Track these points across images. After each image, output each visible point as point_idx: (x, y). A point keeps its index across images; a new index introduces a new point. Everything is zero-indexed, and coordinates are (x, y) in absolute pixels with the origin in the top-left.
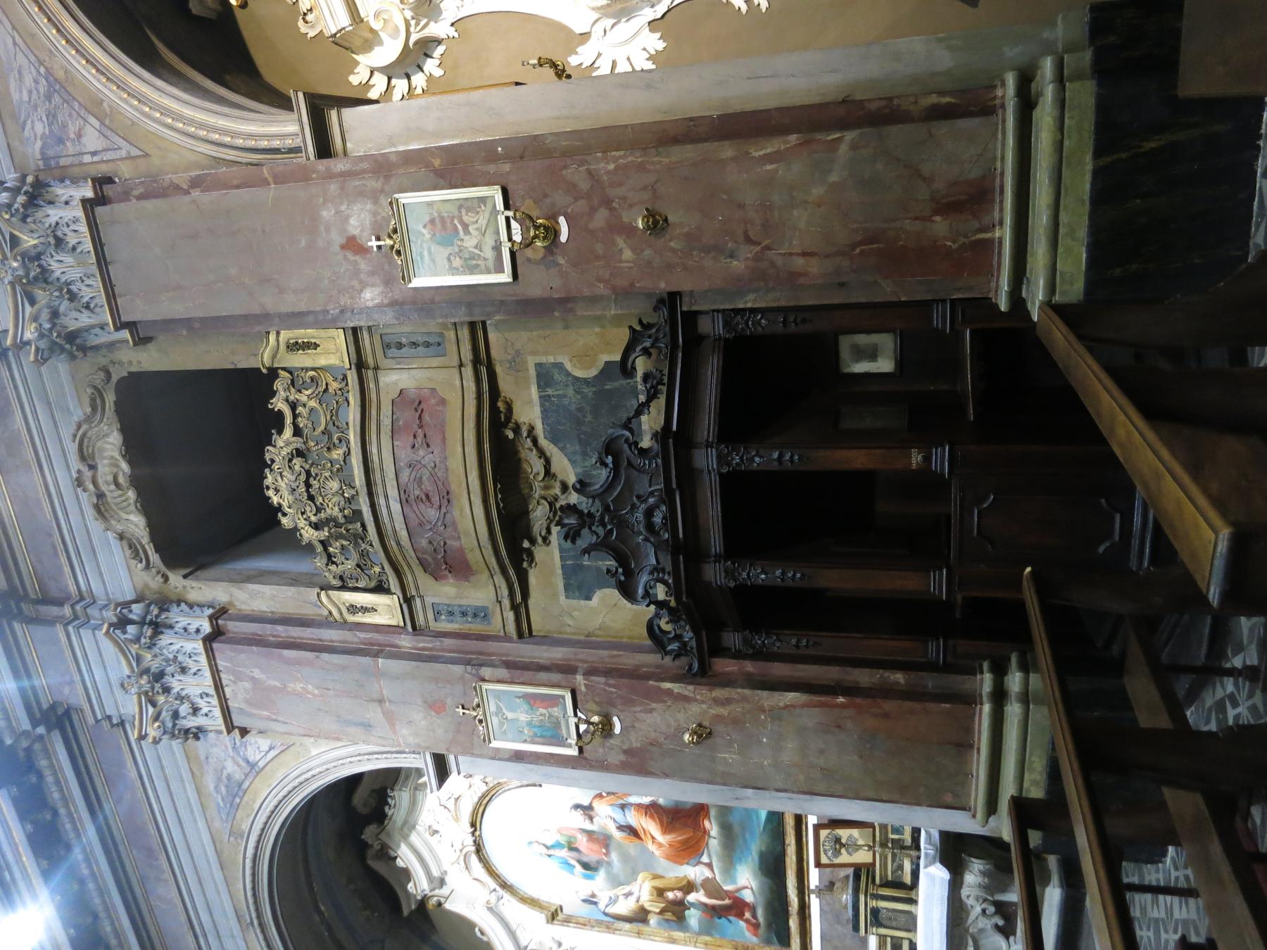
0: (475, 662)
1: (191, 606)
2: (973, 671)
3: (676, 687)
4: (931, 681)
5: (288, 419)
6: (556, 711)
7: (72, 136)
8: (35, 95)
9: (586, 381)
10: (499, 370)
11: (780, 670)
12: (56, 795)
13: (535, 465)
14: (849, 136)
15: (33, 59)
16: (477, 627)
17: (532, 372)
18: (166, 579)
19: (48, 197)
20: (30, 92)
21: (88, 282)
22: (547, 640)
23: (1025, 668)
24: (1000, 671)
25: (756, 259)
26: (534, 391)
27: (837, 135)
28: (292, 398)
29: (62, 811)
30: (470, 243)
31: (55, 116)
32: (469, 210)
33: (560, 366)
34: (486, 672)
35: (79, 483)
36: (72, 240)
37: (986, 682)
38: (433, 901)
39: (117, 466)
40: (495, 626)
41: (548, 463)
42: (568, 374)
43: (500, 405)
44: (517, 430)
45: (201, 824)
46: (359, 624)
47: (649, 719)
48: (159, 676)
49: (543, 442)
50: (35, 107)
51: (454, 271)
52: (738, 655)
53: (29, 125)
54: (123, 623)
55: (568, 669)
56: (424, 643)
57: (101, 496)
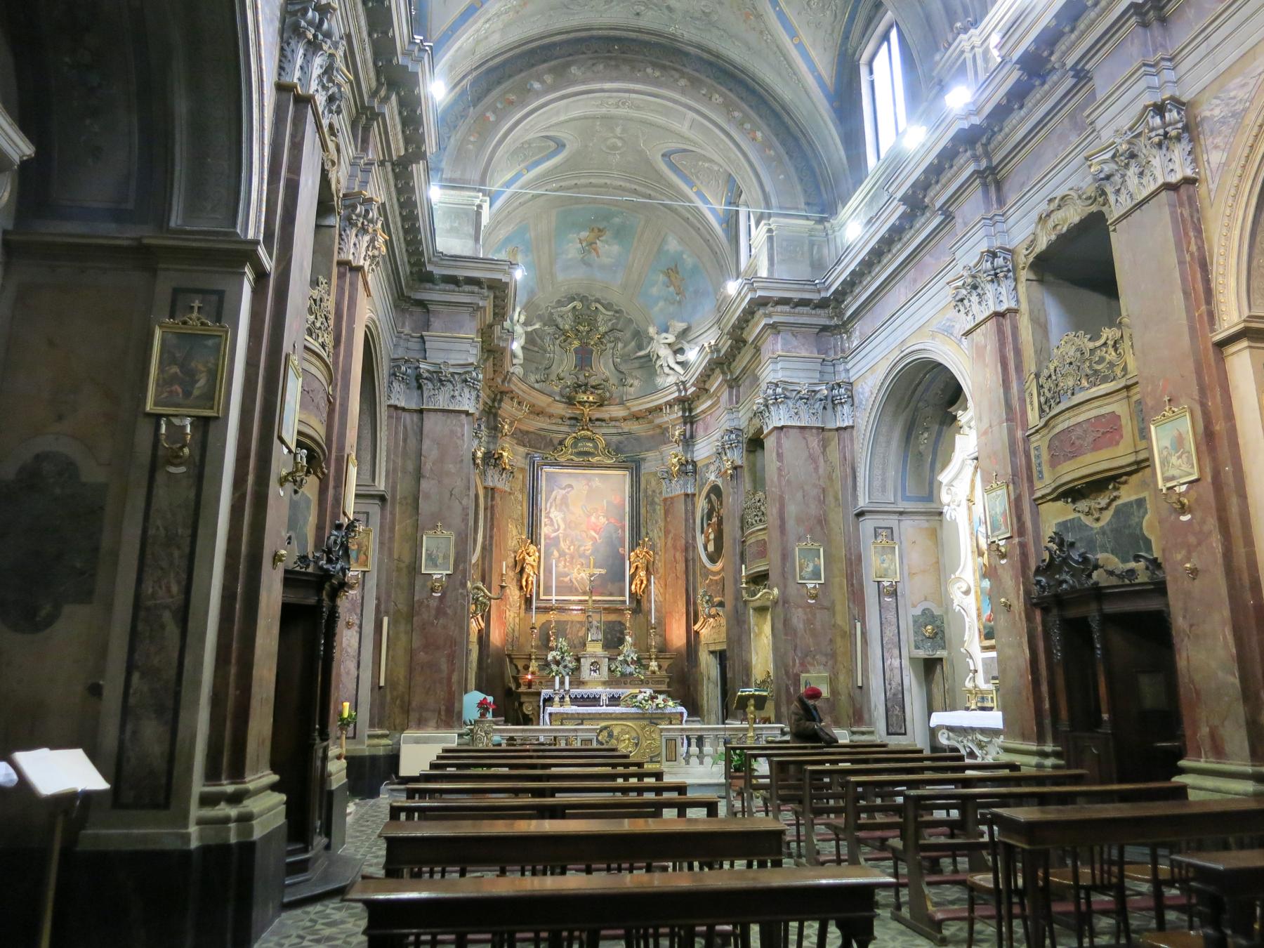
0: (1015, 479)
1: (1015, 288)
2: (1056, 741)
3: (1021, 592)
4: (1047, 721)
5: (1098, 344)
6: (1003, 528)
7: (1215, 142)
8: (1234, 101)
9: (1141, 529)
10: (1140, 474)
11: (1041, 645)
12: (918, 226)
13: (1103, 501)
14: (1237, 682)
15: (1253, 94)
16: (1035, 474)
17: (1141, 496)
18: (1024, 268)
19: (1172, 147)
20: (1234, 98)
21: (1128, 196)
22: (1036, 515)
23: (1055, 767)
24: (1056, 755)
25: (1184, 631)
26: (1134, 498)
27: (1237, 675)
28: (1109, 342)
29: (912, 231)
30: (1174, 460)
31: (1224, 123)
32: (1187, 457)
33: (1146, 512)
34: (1011, 487)
35: (1051, 201)
36: (1144, 181)
37: (1049, 748)
38: (960, 424)
39: (1064, 223)
40: (1038, 485)
41: (1106, 509)
42: (1143, 517)
43: (1124, 478)
44: (1115, 489)
45: (933, 312)
46: (1025, 401)
47: (1009, 578)
48: (975, 287)
49: (1115, 504)
50: (1227, 105)
51: (1160, 453)
52: (1044, 623)
53: (1218, 102)
54: (994, 255)
55: (1021, 531)
56: (1020, 444)
57: (1048, 215)
